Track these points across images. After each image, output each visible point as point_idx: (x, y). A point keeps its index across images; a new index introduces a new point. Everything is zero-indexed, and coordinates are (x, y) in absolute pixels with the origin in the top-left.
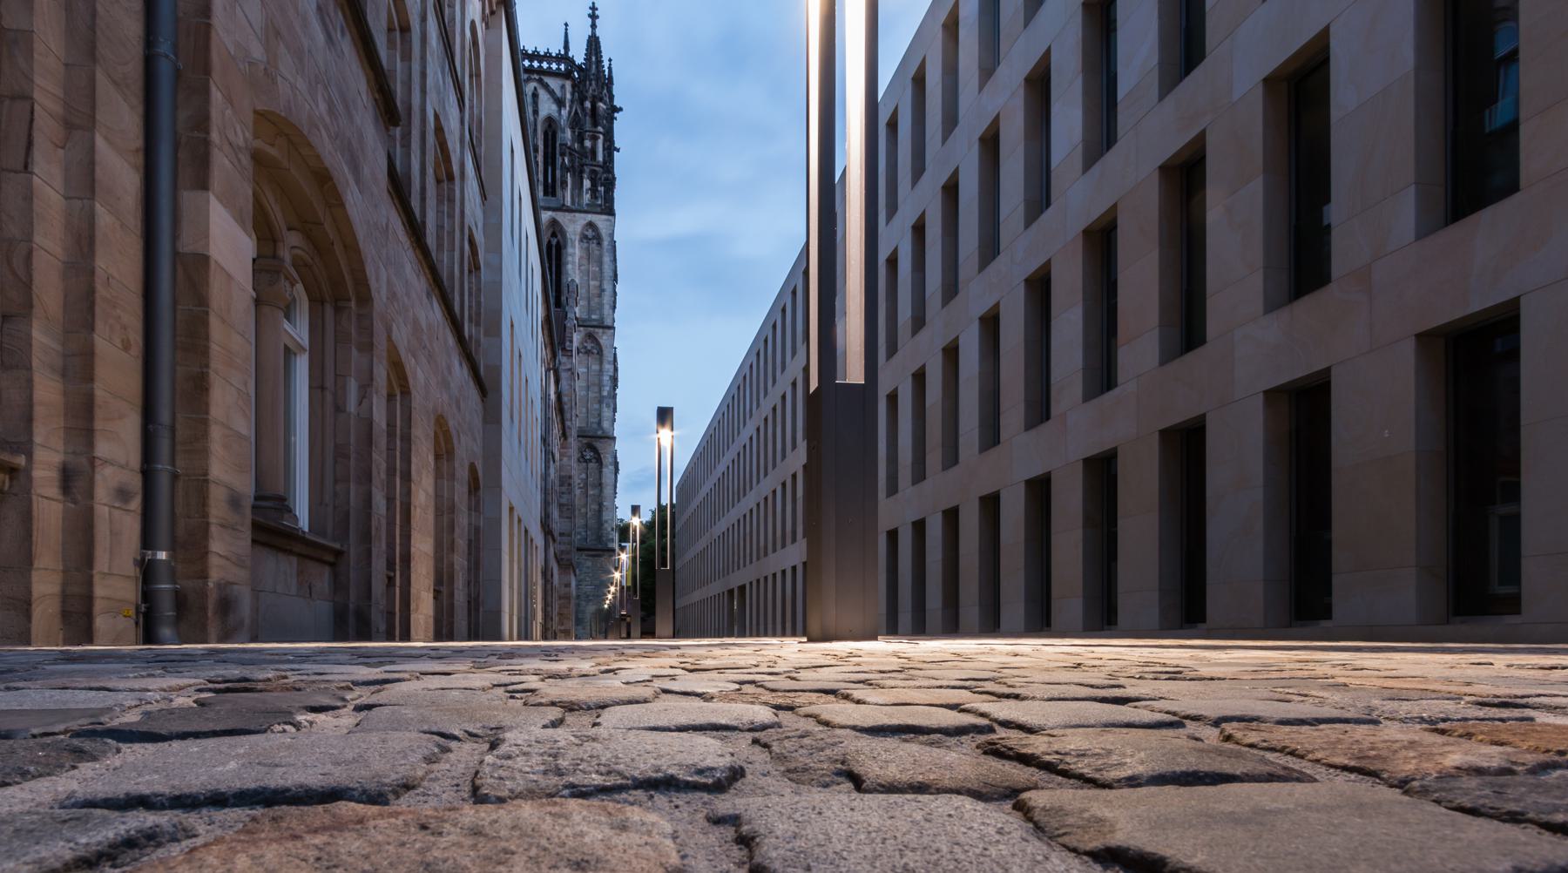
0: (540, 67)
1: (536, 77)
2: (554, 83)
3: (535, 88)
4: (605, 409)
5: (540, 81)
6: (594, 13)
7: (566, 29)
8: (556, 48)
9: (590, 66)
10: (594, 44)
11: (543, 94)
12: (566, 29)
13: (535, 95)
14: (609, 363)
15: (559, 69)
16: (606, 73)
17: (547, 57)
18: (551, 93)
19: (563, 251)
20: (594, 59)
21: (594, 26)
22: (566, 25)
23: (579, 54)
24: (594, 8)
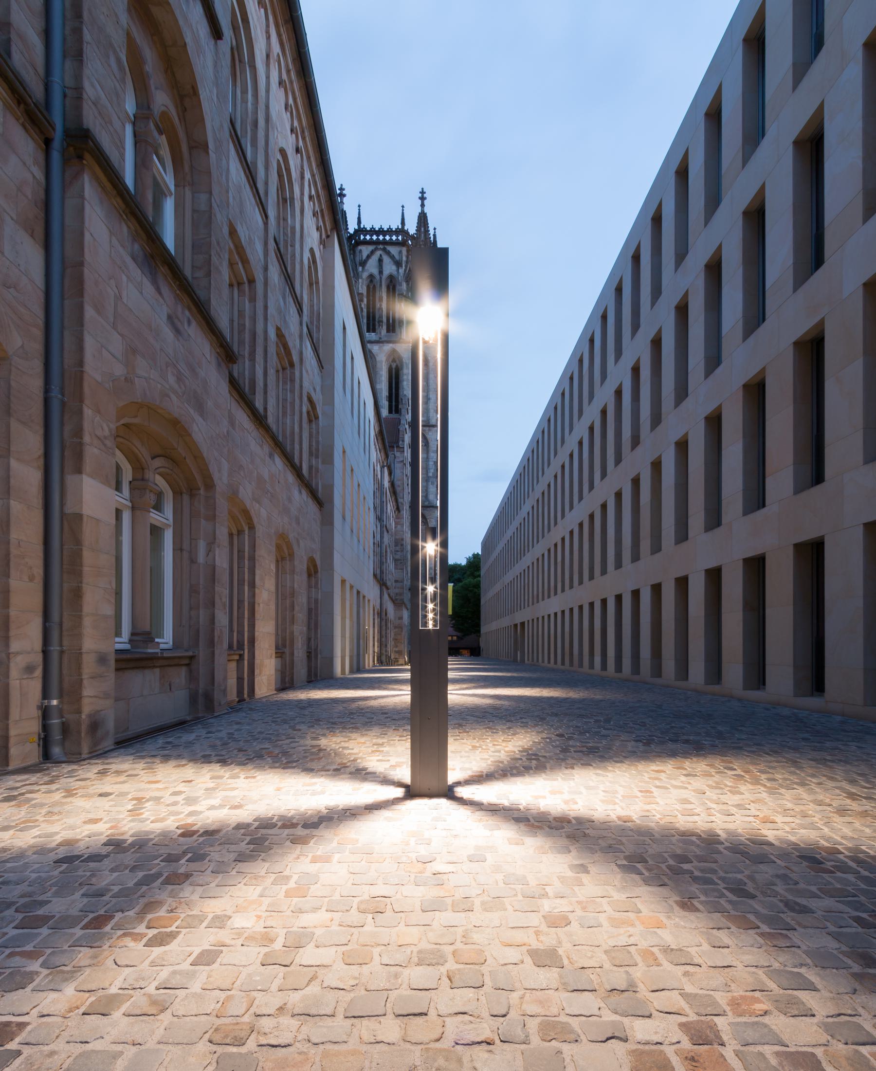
0: (384, 239)
1: (381, 246)
2: (394, 250)
3: (381, 255)
4: (431, 486)
5: (384, 250)
6: (423, 196)
7: (403, 210)
8: (395, 224)
9: (420, 235)
10: (423, 219)
11: (386, 259)
12: (403, 210)
13: (380, 260)
14: (433, 452)
15: (397, 239)
16: (432, 239)
17: (390, 232)
18: (392, 257)
19: (401, 372)
20: (423, 229)
21: (423, 205)
22: (403, 207)
23: (412, 227)
24: (423, 192)
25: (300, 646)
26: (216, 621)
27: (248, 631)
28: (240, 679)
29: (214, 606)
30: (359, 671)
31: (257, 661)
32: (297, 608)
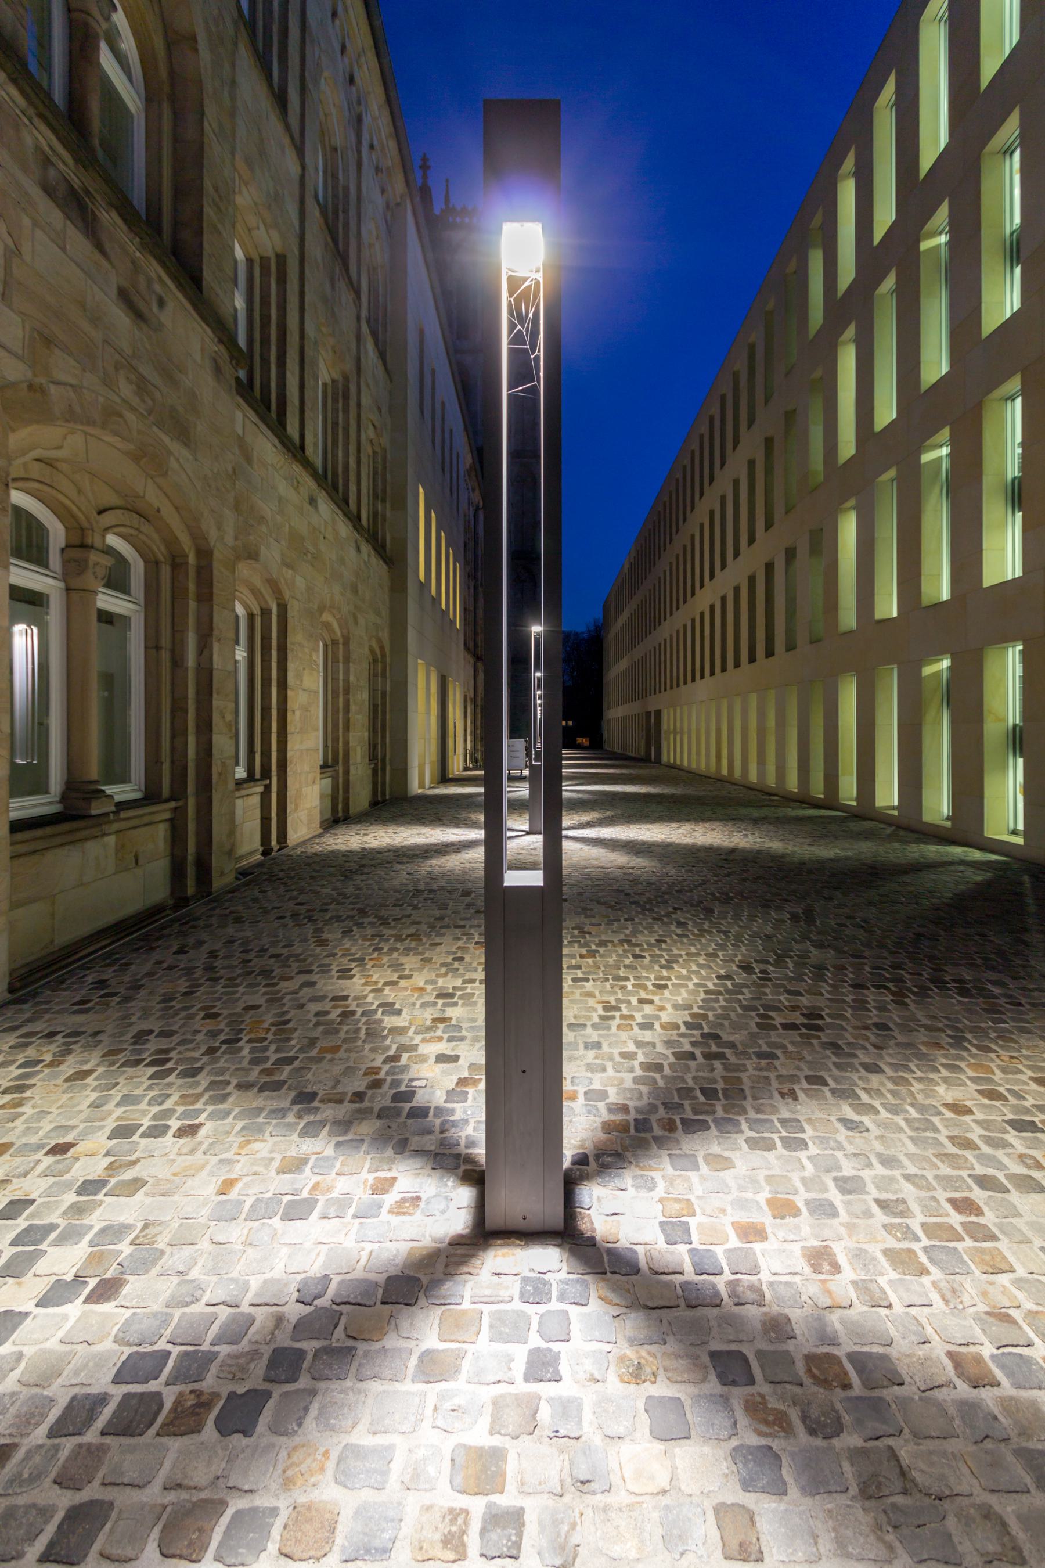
25: (359, 759)
26: (215, 751)
27: (278, 751)
28: (265, 820)
29: (211, 730)
30: (444, 778)
31: (291, 793)
32: (353, 708)
